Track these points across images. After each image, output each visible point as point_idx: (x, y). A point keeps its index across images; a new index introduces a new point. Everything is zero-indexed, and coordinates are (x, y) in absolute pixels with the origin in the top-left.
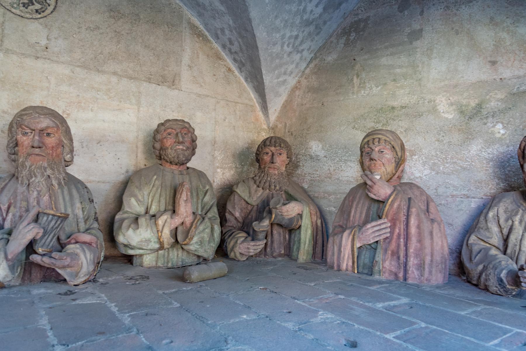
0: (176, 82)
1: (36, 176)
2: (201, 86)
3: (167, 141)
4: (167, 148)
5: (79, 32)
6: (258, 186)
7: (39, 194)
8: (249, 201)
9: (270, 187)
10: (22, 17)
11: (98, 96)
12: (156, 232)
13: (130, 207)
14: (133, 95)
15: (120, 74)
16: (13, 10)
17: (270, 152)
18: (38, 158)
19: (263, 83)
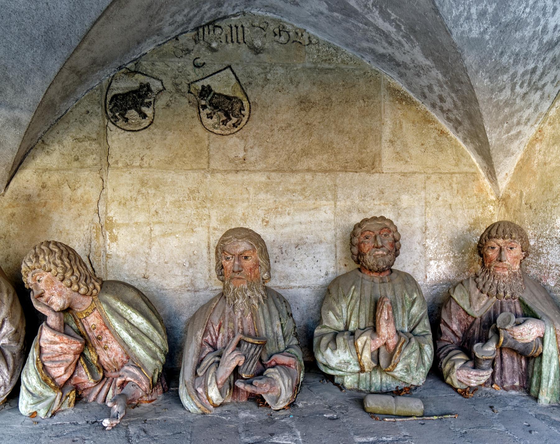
0: (377, 164)
1: (238, 298)
2: (407, 162)
3: (364, 246)
4: (365, 254)
5: (272, 135)
6: (482, 292)
7: (242, 314)
8: (469, 311)
9: (497, 293)
10: (222, 135)
11: (294, 198)
12: (355, 354)
13: (328, 322)
14: (329, 190)
15: (314, 169)
16: (215, 131)
17: (496, 246)
18: (239, 281)
19: (488, 143)
